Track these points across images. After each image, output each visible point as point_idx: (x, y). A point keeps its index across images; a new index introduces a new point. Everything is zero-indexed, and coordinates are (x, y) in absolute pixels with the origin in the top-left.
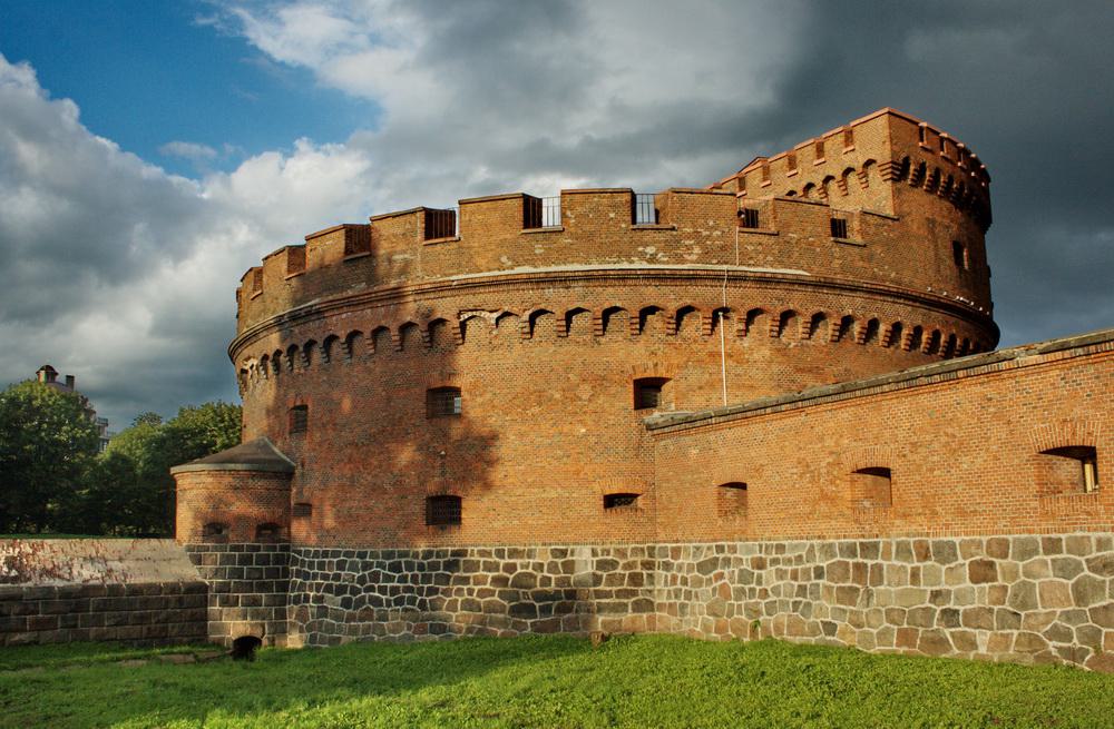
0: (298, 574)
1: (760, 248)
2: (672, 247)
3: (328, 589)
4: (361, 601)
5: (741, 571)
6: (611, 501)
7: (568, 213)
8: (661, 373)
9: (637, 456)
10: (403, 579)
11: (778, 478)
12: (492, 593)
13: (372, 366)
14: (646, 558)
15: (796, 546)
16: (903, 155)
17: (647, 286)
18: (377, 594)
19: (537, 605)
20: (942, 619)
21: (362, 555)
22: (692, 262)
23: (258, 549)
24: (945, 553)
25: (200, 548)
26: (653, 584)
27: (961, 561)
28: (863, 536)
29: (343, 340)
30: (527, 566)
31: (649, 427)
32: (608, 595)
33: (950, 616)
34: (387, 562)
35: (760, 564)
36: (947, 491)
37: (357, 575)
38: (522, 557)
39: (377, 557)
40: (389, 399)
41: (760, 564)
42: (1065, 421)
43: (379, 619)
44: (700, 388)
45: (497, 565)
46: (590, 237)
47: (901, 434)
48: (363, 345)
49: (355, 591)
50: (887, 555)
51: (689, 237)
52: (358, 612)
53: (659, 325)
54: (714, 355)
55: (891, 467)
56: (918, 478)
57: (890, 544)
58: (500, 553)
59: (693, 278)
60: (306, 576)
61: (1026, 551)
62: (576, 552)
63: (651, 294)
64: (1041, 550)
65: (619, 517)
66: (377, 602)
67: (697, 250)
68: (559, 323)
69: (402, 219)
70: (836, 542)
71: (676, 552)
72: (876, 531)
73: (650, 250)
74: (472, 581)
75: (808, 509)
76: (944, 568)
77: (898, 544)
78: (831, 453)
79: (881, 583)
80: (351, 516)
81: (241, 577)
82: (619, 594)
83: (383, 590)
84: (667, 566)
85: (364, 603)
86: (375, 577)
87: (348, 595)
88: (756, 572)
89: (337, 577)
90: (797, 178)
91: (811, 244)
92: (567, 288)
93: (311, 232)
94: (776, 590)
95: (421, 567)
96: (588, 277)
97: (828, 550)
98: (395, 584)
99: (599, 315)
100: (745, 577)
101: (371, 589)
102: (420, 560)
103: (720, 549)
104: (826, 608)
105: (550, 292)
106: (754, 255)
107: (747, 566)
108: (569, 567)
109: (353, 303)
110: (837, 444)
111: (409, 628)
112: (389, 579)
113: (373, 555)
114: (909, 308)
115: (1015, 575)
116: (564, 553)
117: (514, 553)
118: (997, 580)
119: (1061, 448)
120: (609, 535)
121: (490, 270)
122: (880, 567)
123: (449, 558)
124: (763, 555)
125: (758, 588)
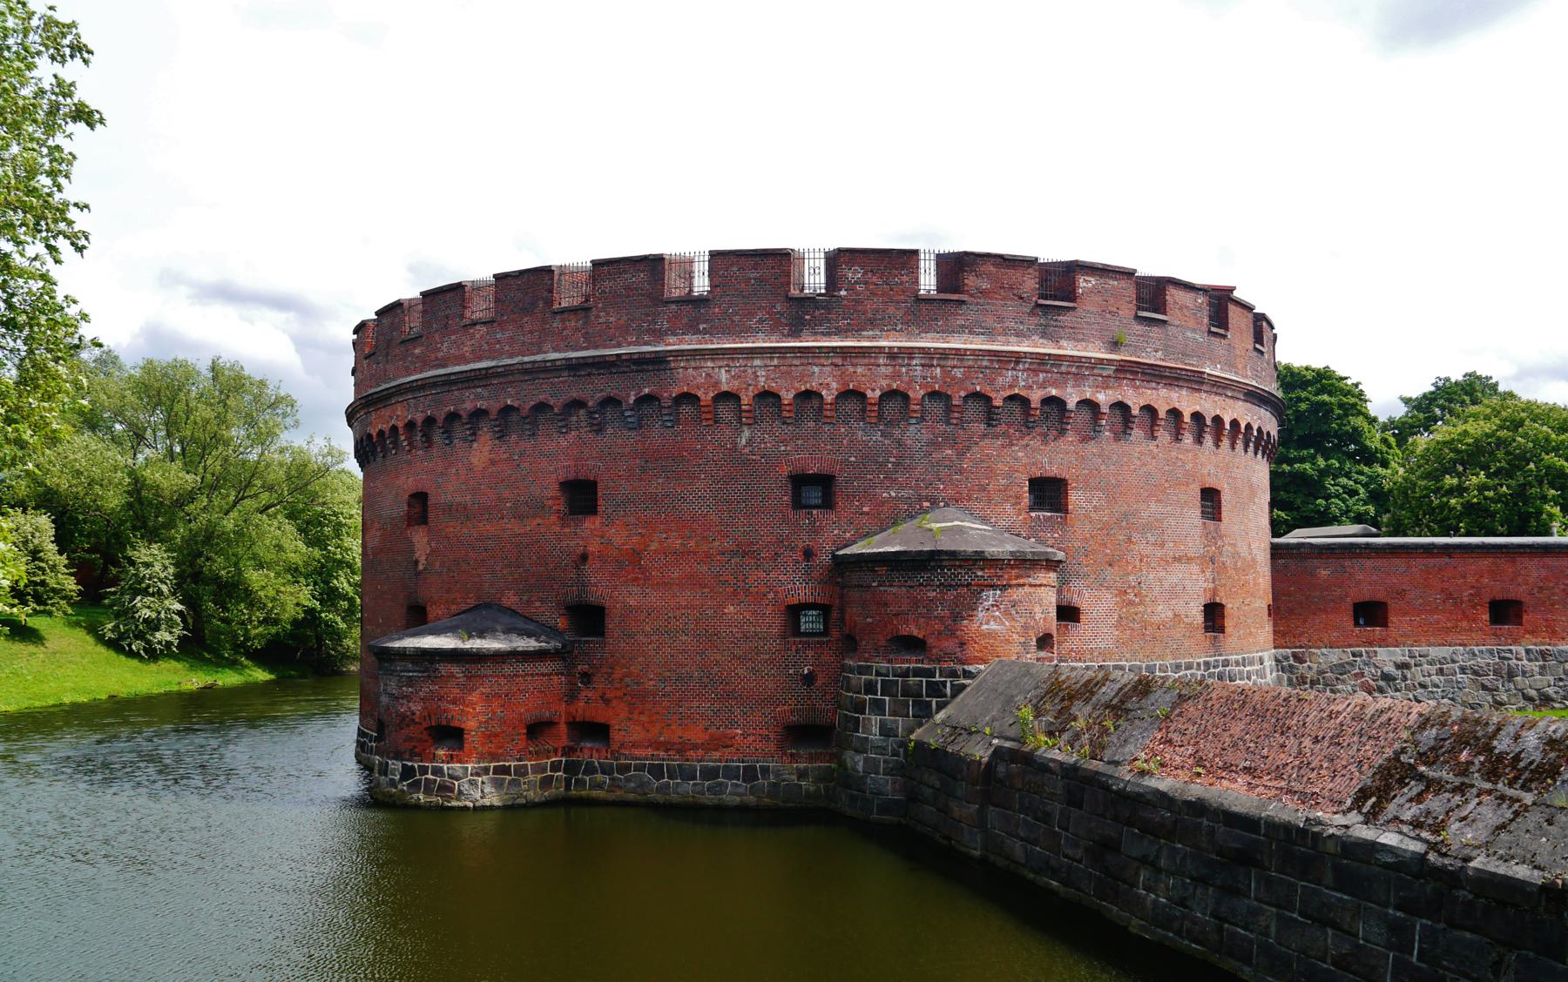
35: (1403, 666)
47: (1531, 580)
109: (1154, 374)
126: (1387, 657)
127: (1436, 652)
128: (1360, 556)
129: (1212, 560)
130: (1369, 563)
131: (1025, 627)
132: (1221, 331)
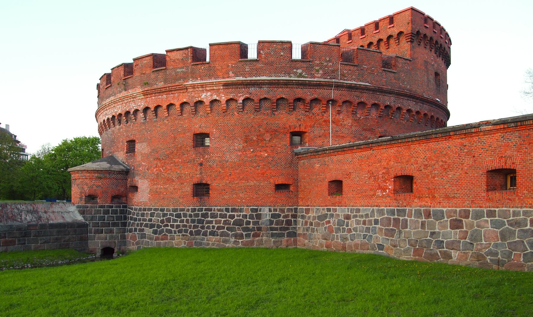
0: (131, 219)
1: (350, 72)
2: (309, 70)
3: (146, 226)
4: (162, 231)
5: (339, 220)
6: (279, 187)
7: (261, 52)
8: (303, 129)
9: (290, 167)
10: (182, 221)
11: (358, 179)
12: (223, 228)
13: (167, 122)
14: (293, 213)
15: (365, 209)
16: (417, 30)
17: (297, 88)
18: (169, 228)
19: (244, 233)
20: (435, 245)
21: (162, 210)
22: (318, 77)
23: (112, 207)
24: (439, 216)
25: (84, 207)
26: (296, 225)
27: (446, 219)
28: (398, 206)
29: (153, 109)
30: (240, 216)
31: (297, 154)
32: (276, 229)
33: (440, 244)
34: (175, 213)
35: (348, 217)
36: (441, 187)
37: (160, 219)
38: (237, 212)
39: (170, 211)
40: (175, 138)
41: (348, 217)
42: (502, 157)
43: (171, 239)
44: (320, 137)
45: (226, 215)
46: (271, 64)
47: (420, 161)
48: (162, 112)
49: (159, 226)
50: (410, 216)
51: (317, 66)
52: (160, 236)
53: (302, 107)
54: (327, 122)
55: (414, 175)
56: (427, 181)
57: (412, 210)
58: (227, 210)
59: (319, 85)
60: (135, 220)
61: (478, 216)
62: (262, 210)
63: (300, 92)
64: (485, 215)
65: (282, 195)
66: (170, 232)
67: (321, 72)
68: (256, 104)
69: (181, 52)
70: (385, 208)
71: (307, 211)
72: (405, 204)
73: (299, 71)
74: (214, 222)
75: (372, 193)
76: (437, 222)
77: (415, 210)
78: (385, 168)
79: (407, 228)
80: (157, 192)
81: (104, 220)
82: (281, 229)
83: (172, 226)
84: (303, 217)
85: (164, 232)
86: (169, 220)
87: (156, 228)
88: (346, 221)
89: (150, 220)
90: (365, 39)
91: (373, 71)
92: (260, 88)
93: (136, 56)
94: (355, 229)
95: (190, 216)
96: (271, 83)
97: (381, 212)
98: (178, 223)
99: (275, 101)
100: (340, 223)
101: (167, 226)
102: (190, 213)
103: (329, 210)
104: (380, 238)
105: (252, 89)
106: (346, 75)
107: (342, 218)
108: (259, 216)
109: (160, 91)
110: (388, 164)
111: (185, 244)
112: (175, 221)
113: (168, 210)
114: (414, 103)
115: (472, 226)
116: (256, 210)
117: (233, 210)
118: (463, 228)
119: (499, 169)
120: (277, 202)
121: (224, 78)
122: (406, 220)
123: (204, 212)
124: (349, 213)
125: (346, 228)
126: (341, 211)
127: (364, 210)
128: (330, 155)
129: (201, 164)
130: (335, 158)
131: (81, 193)
132: (201, 63)
